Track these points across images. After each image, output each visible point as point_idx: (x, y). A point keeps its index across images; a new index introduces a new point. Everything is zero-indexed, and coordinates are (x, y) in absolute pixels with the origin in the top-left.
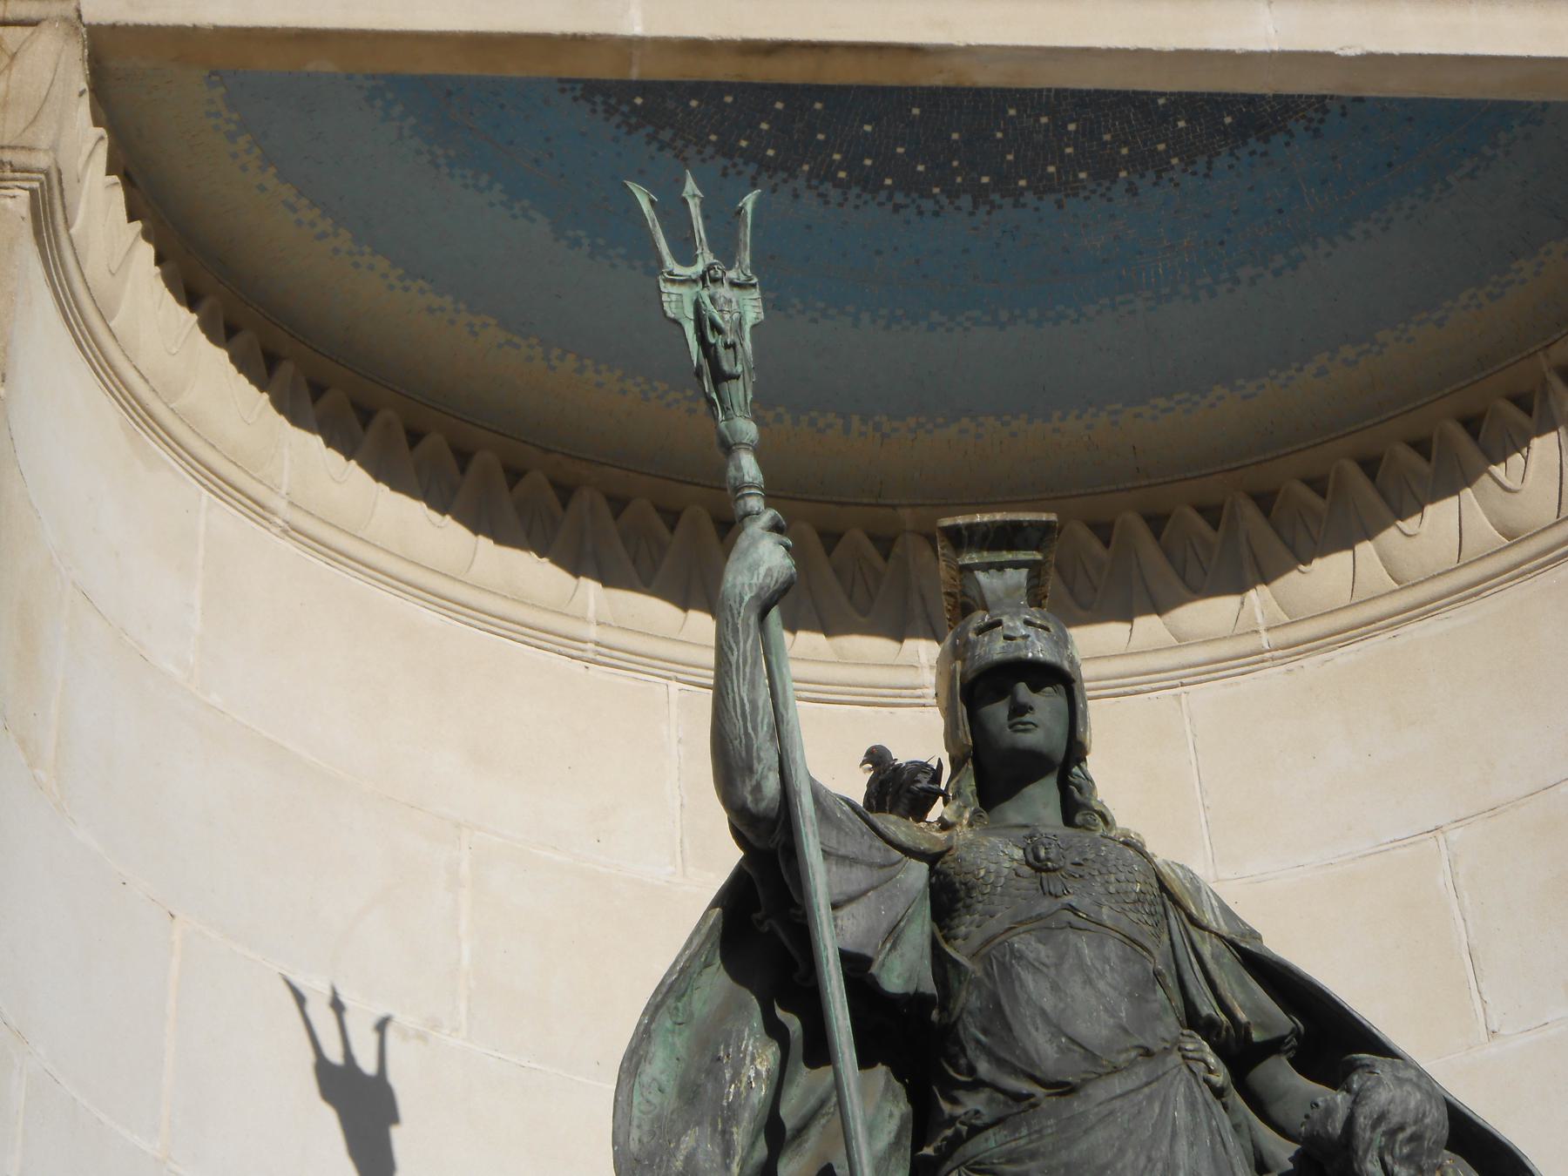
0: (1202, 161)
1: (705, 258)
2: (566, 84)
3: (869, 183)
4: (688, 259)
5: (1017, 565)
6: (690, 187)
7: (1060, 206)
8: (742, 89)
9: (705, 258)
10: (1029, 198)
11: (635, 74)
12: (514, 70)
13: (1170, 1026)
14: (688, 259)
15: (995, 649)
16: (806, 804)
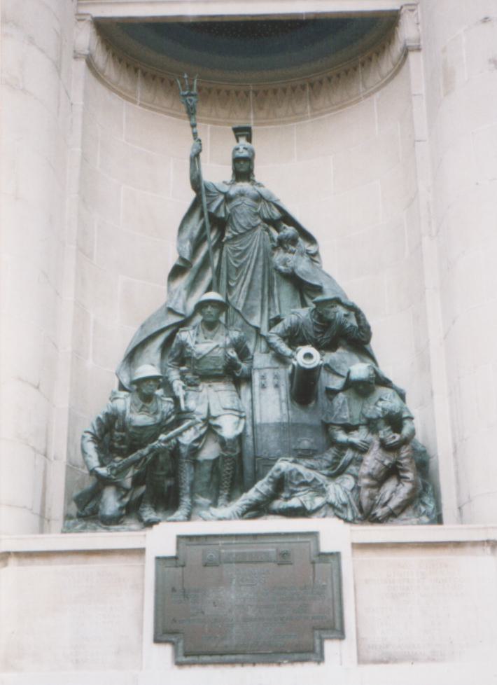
13: (259, 221)
16: (203, 188)
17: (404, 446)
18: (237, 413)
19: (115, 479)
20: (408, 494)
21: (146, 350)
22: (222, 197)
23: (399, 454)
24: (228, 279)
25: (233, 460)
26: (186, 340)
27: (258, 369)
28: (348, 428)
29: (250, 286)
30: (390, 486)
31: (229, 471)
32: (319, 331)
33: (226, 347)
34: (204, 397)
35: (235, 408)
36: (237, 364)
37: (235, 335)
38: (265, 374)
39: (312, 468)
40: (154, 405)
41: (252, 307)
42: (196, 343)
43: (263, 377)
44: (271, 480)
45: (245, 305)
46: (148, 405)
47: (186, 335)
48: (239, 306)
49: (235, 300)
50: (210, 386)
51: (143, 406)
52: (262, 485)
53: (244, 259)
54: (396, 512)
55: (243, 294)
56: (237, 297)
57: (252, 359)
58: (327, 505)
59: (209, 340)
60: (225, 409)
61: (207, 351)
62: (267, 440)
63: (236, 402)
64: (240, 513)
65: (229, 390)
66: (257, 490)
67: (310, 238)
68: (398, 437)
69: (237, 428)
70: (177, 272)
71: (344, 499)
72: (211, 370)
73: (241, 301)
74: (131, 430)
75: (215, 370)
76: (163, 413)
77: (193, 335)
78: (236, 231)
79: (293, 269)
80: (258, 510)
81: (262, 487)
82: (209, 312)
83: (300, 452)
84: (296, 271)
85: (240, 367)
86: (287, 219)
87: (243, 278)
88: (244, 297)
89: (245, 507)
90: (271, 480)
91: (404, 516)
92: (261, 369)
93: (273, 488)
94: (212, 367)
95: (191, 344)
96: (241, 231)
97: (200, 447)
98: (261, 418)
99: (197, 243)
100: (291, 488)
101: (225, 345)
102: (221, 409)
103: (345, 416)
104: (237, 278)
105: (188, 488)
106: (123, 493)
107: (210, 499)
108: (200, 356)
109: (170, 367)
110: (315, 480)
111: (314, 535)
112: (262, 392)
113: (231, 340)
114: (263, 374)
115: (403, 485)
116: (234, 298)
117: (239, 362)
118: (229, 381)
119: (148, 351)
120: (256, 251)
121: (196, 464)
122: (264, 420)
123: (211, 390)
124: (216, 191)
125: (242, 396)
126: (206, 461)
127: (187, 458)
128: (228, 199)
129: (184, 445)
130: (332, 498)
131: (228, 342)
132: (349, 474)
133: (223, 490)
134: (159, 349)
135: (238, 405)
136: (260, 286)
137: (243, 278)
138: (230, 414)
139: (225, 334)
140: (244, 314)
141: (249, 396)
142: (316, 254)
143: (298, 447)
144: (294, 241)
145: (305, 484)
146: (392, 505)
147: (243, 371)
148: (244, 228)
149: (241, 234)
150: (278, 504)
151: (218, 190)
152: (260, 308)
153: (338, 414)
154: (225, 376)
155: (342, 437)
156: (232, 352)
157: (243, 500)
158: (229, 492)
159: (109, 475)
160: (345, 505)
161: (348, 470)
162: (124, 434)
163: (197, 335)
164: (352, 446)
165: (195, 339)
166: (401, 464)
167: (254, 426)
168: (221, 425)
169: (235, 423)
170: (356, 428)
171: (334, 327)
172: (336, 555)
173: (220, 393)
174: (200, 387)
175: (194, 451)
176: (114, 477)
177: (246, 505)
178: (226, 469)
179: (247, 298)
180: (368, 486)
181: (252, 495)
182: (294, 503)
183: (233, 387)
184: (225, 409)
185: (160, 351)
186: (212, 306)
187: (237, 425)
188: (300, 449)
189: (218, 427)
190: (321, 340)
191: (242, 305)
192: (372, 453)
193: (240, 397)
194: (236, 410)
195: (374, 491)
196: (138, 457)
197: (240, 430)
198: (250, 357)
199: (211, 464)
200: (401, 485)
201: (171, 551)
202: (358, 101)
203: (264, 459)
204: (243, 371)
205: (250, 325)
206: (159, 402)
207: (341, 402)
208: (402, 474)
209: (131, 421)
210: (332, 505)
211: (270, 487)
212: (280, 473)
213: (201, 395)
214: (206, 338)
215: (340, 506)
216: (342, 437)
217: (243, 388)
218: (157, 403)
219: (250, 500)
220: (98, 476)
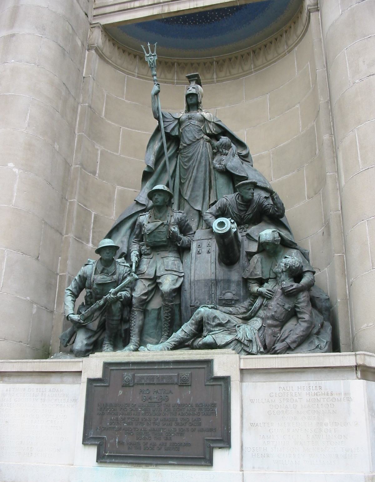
0: (234, 14)
1: (150, 53)
2: (156, 20)
3: (195, 24)
4: (148, 53)
5: (194, 80)
6: (149, 44)
7: (219, 22)
8: (176, 17)
9: (150, 53)
10: (215, 22)
11: (163, 18)
12: (150, 20)
14: (148, 53)
15: (189, 92)
16: (161, 116)
17: (301, 293)
20: (303, 331)
22: (176, 122)
23: (297, 299)
25: (171, 308)
26: (143, 221)
28: (261, 282)
30: (291, 324)
32: (242, 209)
35: (175, 269)
36: (177, 236)
39: (230, 313)
43: (199, 246)
45: (191, 195)
48: (187, 196)
51: (104, 269)
53: (191, 162)
54: (293, 346)
58: (235, 342)
60: (166, 270)
66: (183, 330)
67: (240, 144)
68: (295, 285)
69: (174, 284)
70: (146, 176)
71: (249, 337)
73: (189, 193)
74: (95, 286)
77: (148, 217)
78: (185, 143)
79: (225, 166)
80: (180, 345)
81: (187, 327)
83: (224, 302)
84: (227, 167)
86: (225, 132)
91: (299, 349)
95: (145, 223)
96: (188, 142)
99: (160, 155)
100: (209, 327)
103: (258, 273)
108: (150, 232)
109: (134, 242)
110: (229, 321)
111: (209, 363)
115: (300, 324)
117: (179, 235)
120: (199, 155)
124: (173, 118)
128: (180, 122)
129: (135, 298)
130: (240, 335)
132: (258, 317)
142: (247, 156)
143: (223, 298)
144: (228, 147)
145: (220, 325)
146: (288, 341)
147: (183, 242)
148: (191, 141)
149: (189, 145)
150: (200, 341)
151: (173, 117)
153: (252, 271)
155: (255, 288)
156: (174, 228)
157: (172, 338)
158: (169, 333)
159: (79, 320)
160: (250, 341)
161: (258, 314)
162: (91, 291)
164: (260, 294)
166: (298, 307)
170: (267, 281)
171: (254, 205)
172: (226, 380)
173: (165, 259)
175: (144, 303)
176: (82, 322)
180: (270, 326)
181: (179, 334)
182: (208, 339)
184: (166, 270)
187: (175, 281)
188: (224, 300)
189: (160, 283)
190: (244, 216)
192: (275, 299)
195: (277, 330)
196: (97, 306)
197: (178, 285)
198: (192, 232)
200: (298, 324)
201: (99, 374)
202: (285, 55)
204: (183, 242)
207: (256, 261)
208: (300, 316)
209: (94, 280)
210: (239, 341)
211: (193, 328)
212: (200, 315)
215: (246, 342)
216: (255, 288)
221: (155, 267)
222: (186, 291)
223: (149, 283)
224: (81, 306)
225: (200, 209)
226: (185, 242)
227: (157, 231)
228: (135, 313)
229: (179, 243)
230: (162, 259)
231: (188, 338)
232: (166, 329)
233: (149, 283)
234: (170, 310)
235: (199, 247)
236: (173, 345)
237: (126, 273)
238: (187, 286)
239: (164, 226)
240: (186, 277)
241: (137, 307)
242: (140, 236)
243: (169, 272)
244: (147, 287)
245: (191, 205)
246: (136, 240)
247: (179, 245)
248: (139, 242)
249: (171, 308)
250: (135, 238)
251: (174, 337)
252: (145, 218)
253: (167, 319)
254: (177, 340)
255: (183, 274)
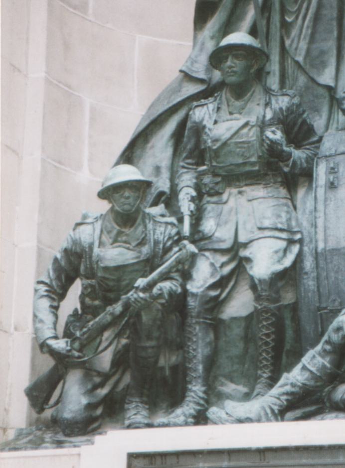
18: (284, 235)
19: (79, 357)
21: (149, 145)
24: (283, 11)
25: (273, 315)
27: (326, 156)
29: (317, 18)
31: (267, 335)
33: (263, 125)
34: (231, 211)
35: (280, 226)
36: (283, 151)
37: (283, 102)
38: (338, 164)
40: (141, 228)
41: (323, 53)
42: (216, 122)
44: (328, 347)
45: (308, 52)
46: (126, 231)
47: (203, 113)
48: (300, 55)
49: (294, 46)
50: (240, 193)
51: (119, 233)
52: (314, 357)
55: (306, 32)
56: (296, 42)
57: (320, 139)
59: (236, 116)
60: (260, 229)
61: (228, 135)
62: (336, 279)
63: (284, 215)
64: (276, 408)
65: (272, 197)
66: (304, 368)
69: (279, 261)
72: (238, 165)
73: (303, 45)
74: (100, 274)
75: (244, 164)
76: (156, 243)
77: (213, 110)
82: (230, 67)
85: (290, 155)
87: (305, 5)
88: (308, 38)
89: (284, 398)
90: (328, 347)
92: (330, 156)
93: (330, 362)
94: (240, 161)
95: (208, 123)
97: (224, 295)
98: (326, 241)
101: (263, 122)
102: (255, 229)
104: (295, 9)
105: (200, 368)
106: (97, 380)
107: (245, 385)
108: (218, 144)
109: (183, 167)
112: (331, 194)
113: (275, 113)
114: (332, 165)
116: (293, 41)
117: (286, 149)
118: (275, 182)
119: (153, 147)
121: (217, 326)
122: (331, 245)
123: (243, 200)
125: (299, 204)
126: (234, 319)
127: (198, 317)
129: (194, 295)
131: (269, 115)
133: (261, 369)
134: (169, 141)
135: (289, 220)
136: (335, 14)
137: (305, 5)
138: (270, 237)
139: (262, 102)
140: (307, 68)
141: (310, 204)
147: (294, 163)
152: (335, 52)
154: (266, 175)
156: (274, 132)
157: (282, 386)
158: (272, 371)
159: (69, 351)
162: (93, 282)
163: (219, 109)
165: (214, 117)
167: (317, 255)
168: (251, 256)
169: (276, 252)
173: (255, 202)
174: (225, 197)
175: (214, 305)
176: (76, 354)
177: (287, 394)
178: (264, 330)
179: (312, 39)
183: (283, 192)
184: (260, 229)
185: (171, 143)
186: (236, 57)
187: (281, 254)
189: (248, 260)
191: (303, 53)
193: (295, 208)
194: (281, 230)
196: (109, 318)
197: (288, 261)
198: (315, 139)
199: (243, 324)
203: (331, 311)
204: (294, 163)
205: (319, 85)
206: (150, 226)
209: (100, 259)
211: (326, 362)
213: (226, 208)
214: (231, 113)
217: (301, 193)
218: (145, 226)
219: (293, 385)
220: (52, 352)
221: (234, 222)
222: (306, 273)
223: (224, 259)
224: (72, 319)
225: (332, 84)
226: (299, 162)
227: (233, 141)
228: (195, 329)
229: (287, 166)
230: (250, 203)
231: (319, 384)
232: (265, 363)
233: (224, 259)
234: (274, 319)
235: (332, 171)
236: (285, 403)
237: (169, 238)
238: (308, 264)
239: (250, 130)
240: (307, 240)
241: (198, 317)
242: (196, 153)
243: (268, 233)
244: (218, 269)
245: (311, 75)
246: (189, 161)
247: (286, 169)
248: (195, 167)
249: (273, 315)
250: (187, 158)
251: (286, 385)
252: (207, 112)
253: (268, 340)
254: (293, 390)
255: (298, 236)
